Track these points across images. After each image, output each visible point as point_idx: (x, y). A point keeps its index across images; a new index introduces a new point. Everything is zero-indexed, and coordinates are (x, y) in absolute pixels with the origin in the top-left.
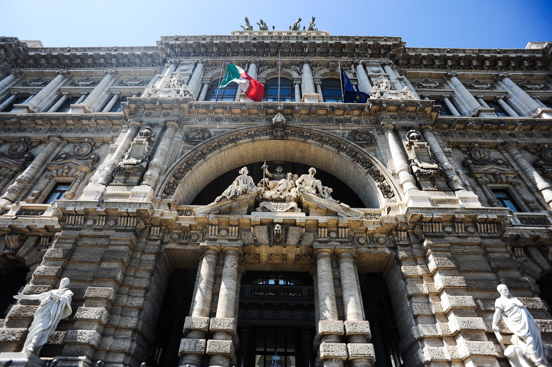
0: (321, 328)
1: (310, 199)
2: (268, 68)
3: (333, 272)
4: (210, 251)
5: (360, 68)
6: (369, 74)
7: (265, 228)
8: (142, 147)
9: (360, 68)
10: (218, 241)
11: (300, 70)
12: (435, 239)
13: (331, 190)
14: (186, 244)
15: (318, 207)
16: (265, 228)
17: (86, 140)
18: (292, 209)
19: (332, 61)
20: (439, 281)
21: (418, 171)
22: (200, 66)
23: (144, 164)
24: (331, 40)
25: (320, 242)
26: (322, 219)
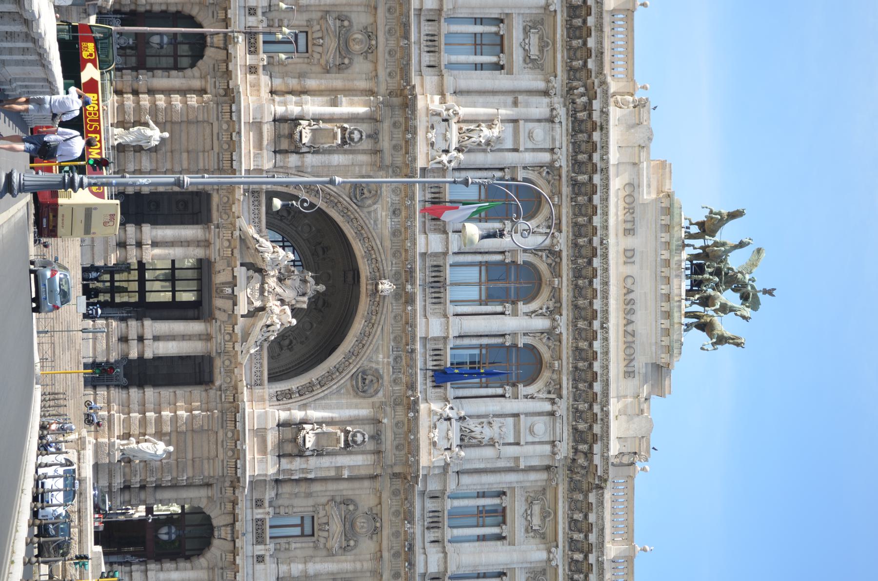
0: (148, 323)
1: (261, 319)
2: (550, 265)
3: (196, 335)
4: (207, 235)
5: (547, 407)
6: (522, 417)
7: (230, 279)
8: (330, 140)
9: (547, 407)
10: (217, 240)
11: (542, 315)
12: (220, 421)
13: (272, 338)
14: (218, 211)
15: (253, 325)
16: (230, 279)
17: (374, 42)
18: (250, 303)
19: (561, 366)
20: (183, 413)
21: (304, 429)
22: (546, 157)
23: (304, 150)
24: (602, 367)
25: (220, 326)
26: (238, 329)
